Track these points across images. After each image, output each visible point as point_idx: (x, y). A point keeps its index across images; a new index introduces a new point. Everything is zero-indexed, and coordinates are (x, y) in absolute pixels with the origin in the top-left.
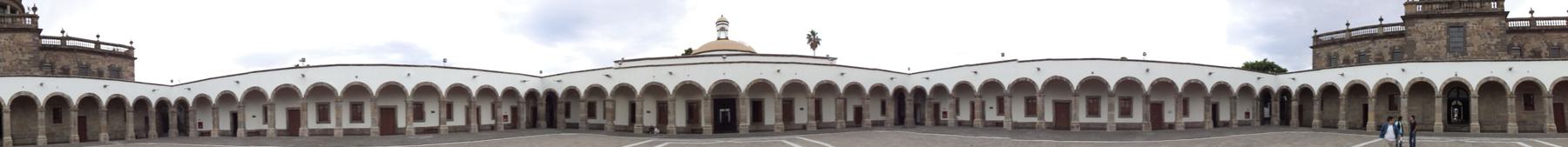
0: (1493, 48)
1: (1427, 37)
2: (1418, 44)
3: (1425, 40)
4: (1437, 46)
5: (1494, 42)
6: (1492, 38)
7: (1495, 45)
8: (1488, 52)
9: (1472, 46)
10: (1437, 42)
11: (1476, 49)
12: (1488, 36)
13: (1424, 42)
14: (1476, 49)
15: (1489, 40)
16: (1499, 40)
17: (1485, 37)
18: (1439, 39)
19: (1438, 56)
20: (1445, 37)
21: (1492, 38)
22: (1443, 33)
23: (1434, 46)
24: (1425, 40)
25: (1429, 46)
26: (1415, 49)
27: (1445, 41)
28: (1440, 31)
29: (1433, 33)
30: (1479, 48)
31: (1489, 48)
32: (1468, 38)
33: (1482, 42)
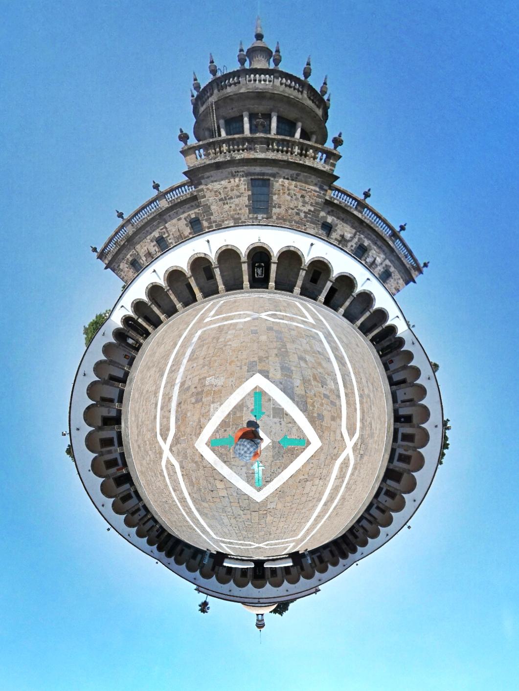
0: (302, 215)
1: (223, 196)
3: (221, 200)
4: (237, 205)
5: (306, 209)
7: (305, 212)
8: (296, 218)
10: (236, 201)
12: (301, 199)
15: (301, 204)
17: (297, 199)
18: (238, 197)
21: (305, 203)
23: (233, 206)
24: (221, 200)
25: (226, 207)
28: (238, 186)
31: (298, 214)
32: (275, 197)
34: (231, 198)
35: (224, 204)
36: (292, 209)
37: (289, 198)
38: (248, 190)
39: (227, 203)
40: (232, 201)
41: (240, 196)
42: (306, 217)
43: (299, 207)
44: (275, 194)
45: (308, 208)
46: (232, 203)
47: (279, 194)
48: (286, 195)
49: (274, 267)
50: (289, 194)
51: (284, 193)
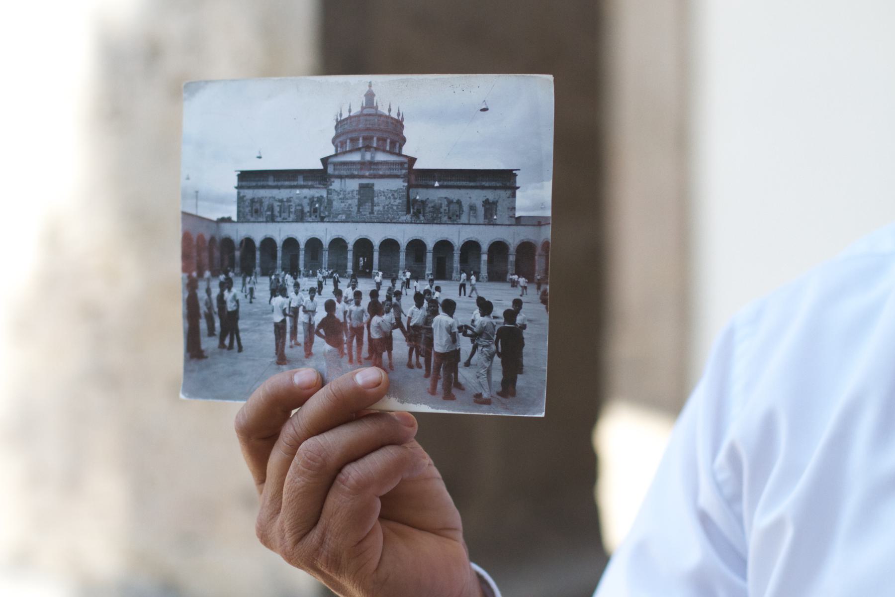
0: (395, 208)
2: (335, 203)
3: (340, 199)
4: (350, 205)
6: (395, 198)
7: (396, 205)
9: (379, 206)
10: (350, 202)
11: (381, 208)
12: (392, 197)
13: (340, 201)
14: (381, 208)
16: (401, 201)
19: (350, 214)
20: (357, 197)
21: (395, 198)
22: (355, 193)
23: (347, 204)
25: (343, 205)
26: (332, 207)
27: (356, 201)
29: (347, 193)
30: (384, 207)
31: (392, 208)
33: (387, 203)
34: (347, 199)
35: (342, 202)
36: (387, 205)
37: (384, 198)
38: (359, 195)
39: (344, 202)
40: (347, 201)
41: (353, 199)
42: (397, 208)
43: (392, 203)
44: (375, 197)
45: (398, 201)
46: (347, 202)
47: (378, 196)
48: (382, 196)
49: (376, 255)
50: (384, 196)
51: (381, 195)
